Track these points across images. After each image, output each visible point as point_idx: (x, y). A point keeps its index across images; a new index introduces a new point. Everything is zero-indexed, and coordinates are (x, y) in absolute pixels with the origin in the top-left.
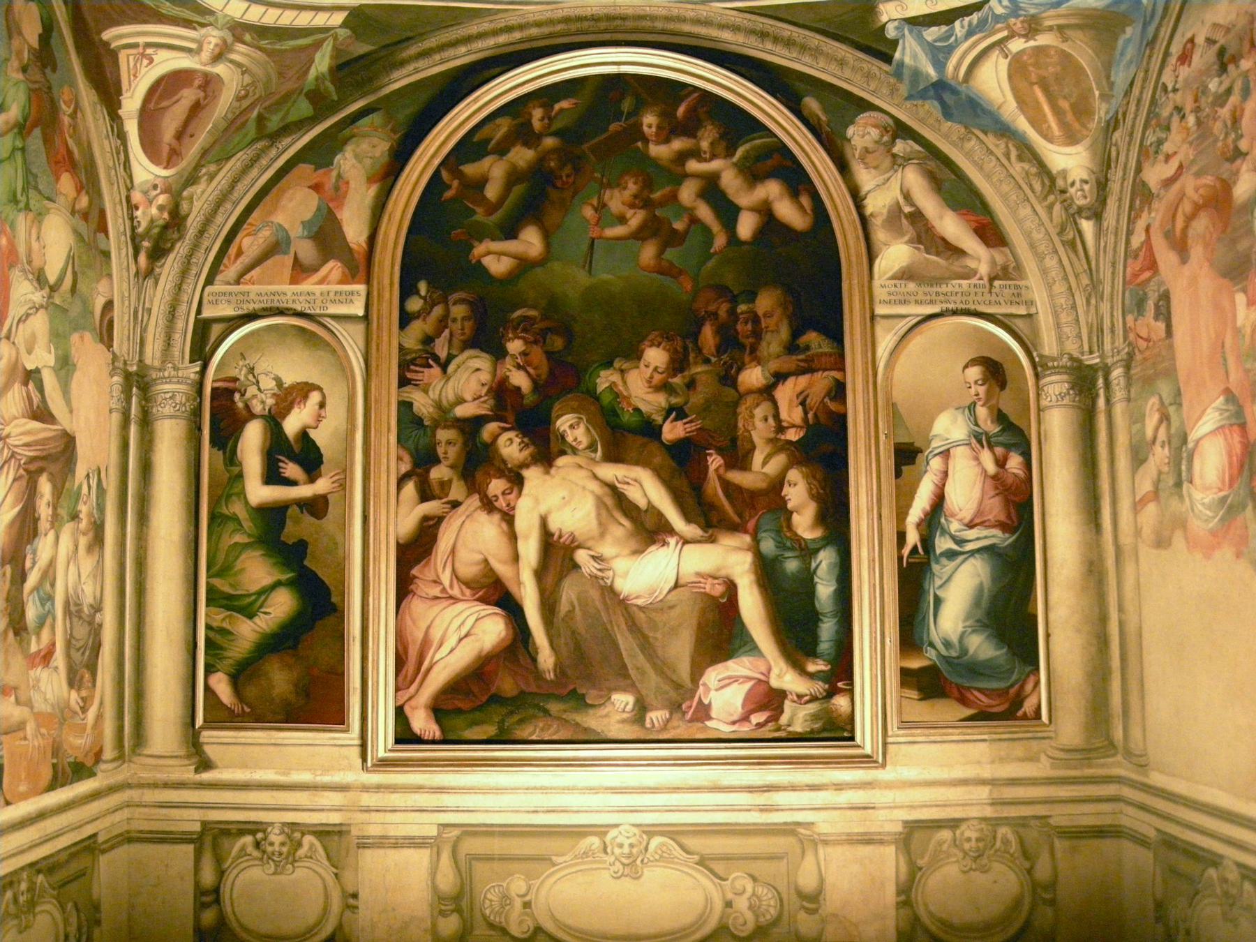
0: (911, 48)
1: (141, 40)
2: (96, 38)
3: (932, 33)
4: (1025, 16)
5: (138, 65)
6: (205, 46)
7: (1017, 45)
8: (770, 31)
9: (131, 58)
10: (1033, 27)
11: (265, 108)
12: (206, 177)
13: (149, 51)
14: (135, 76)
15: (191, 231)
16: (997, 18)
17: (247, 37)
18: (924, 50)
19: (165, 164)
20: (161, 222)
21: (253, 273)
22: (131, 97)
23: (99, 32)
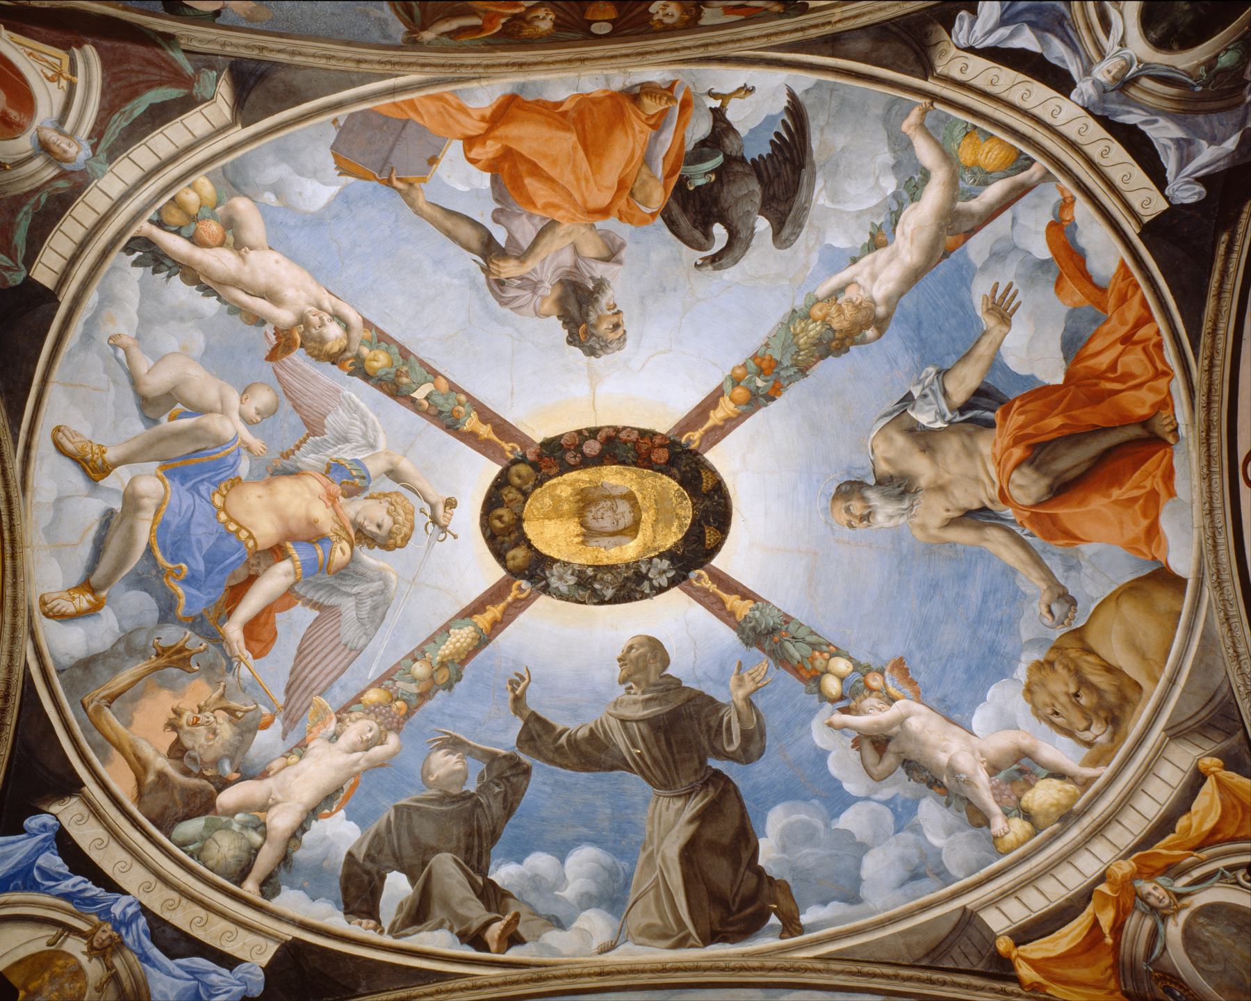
0: (19, 848)
3: (53, 861)
4: (120, 936)
7: (75, 947)
8: (9, 704)
10: (100, 952)
16: (106, 913)
18: (19, 862)
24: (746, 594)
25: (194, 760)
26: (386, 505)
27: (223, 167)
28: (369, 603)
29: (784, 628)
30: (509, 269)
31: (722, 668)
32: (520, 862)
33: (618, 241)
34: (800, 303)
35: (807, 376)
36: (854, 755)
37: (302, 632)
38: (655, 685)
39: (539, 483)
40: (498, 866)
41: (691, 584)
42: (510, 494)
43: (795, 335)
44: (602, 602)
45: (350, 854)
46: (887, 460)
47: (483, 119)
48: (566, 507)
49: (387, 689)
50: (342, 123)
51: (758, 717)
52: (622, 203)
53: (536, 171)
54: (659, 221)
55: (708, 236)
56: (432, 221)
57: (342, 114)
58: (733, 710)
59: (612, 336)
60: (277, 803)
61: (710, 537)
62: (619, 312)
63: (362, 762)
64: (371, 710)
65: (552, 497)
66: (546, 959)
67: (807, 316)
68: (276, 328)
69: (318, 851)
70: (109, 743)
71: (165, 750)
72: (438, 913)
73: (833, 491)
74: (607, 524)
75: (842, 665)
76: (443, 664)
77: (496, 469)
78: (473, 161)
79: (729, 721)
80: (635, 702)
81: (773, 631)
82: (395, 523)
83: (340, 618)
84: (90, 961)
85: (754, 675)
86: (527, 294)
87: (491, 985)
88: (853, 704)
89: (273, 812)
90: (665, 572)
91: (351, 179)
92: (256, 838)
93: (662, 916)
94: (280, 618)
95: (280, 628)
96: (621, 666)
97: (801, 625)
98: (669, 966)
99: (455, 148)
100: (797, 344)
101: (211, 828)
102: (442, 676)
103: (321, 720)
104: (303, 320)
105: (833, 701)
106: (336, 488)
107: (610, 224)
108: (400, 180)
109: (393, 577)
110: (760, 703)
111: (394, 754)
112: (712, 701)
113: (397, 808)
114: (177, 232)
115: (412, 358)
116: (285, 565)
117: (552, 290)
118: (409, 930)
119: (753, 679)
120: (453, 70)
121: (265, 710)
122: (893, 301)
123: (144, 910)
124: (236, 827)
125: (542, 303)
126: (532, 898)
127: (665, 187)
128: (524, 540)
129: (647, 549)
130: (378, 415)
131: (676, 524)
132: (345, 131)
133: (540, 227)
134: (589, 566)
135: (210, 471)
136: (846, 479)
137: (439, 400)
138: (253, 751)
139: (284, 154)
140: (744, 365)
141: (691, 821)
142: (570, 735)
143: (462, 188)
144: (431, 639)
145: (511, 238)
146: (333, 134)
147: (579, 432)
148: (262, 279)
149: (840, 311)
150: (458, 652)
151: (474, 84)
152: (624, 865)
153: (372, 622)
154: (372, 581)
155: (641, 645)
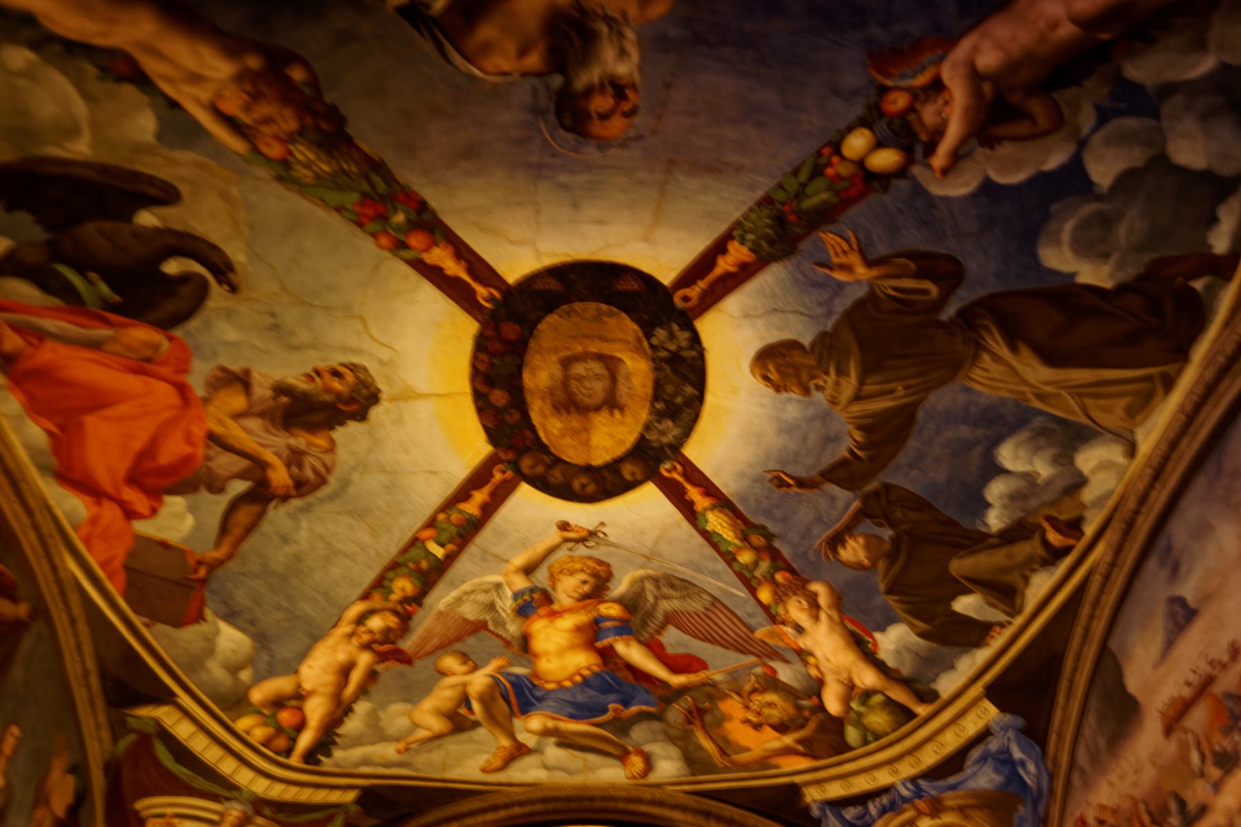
1: (169, 811)
3: (850, 813)
16: (904, 800)
17: (267, 811)
24: (719, 248)
25: (792, 720)
26: (562, 577)
27: (222, 710)
28: (666, 590)
29: (779, 206)
30: (280, 476)
31: (818, 285)
32: (988, 505)
33: (219, 374)
34: (262, 172)
35: (382, 160)
36: (1006, 149)
37: (686, 637)
38: (820, 360)
39: (544, 449)
40: (986, 525)
41: (692, 309)
42: (557, 475)
43: (318, 177)
44: (700, 398)
45: (922, 635)
46: (522, 52)
47: (99, 503)
48: (575, 424)
49: (760, 583)
50: (146, 620)
51: (900, 255)
52: (165, 371)
53: (149, 452)
54: (178, 333)
55: (185, 279)
56: (236, 545)
57: (137, 620)
58: (880, 282)
59: (350, 377)
60: (851, 680)
61: (632, 285)
62: (318, 372)
63: (829, 612)
64: (780, 598)
65: (563, 436)
66: (1111, 503)
67: (285, 163)
68: (378, 662)
69: (908, 658)
70: (764, 762)
71: (776, 734)
72: (1015, 578)
73: (570, 137)
74: (598, 388)
75: (857, 143)
76: (745, 538)
77: (525, 490)
78: (154, 511)
79: (895, 289)
80: (837, 384)
81: (780, 220)
82: (582, 570)
83: (678, 611)
84: (939, 818)
85: (839, 250)
86: (309, 461)
87: (1113, 565)
88: (924, 137)
89: (858, 682)
90: (672, 336)
91: (208, 613)
92: (878, 699)
93: (1121, 395)
94: (670, 650)
95: (681, 651)
96: (786, 390)
97: (780, 186)
98: (1189, 408)
99: (143, 527)
100: (333, 176)
101: (859, 723)
102: (757, 540)
103: (781, 636)
104: (367, 647)
105: (910, 161)
106: (542, 611)
107: (197, 381)
108: (196, 571)
109: (641, 572)
110: (882, 250)
111: (831, 589)
112: (860, 305)
113: (890, 591)
114: (294, 740)
115: (401, 560)
116: (620, 648)
117: (297, 436)
118: (1018, 601)
119: (845, 252)
120: (49, 541)
121: (759, 670)
122: (231, 46)
123: (913, 780)
124: (862, 709)
125: (317, 446)
126: (1033, 503)
127: (124, 326)
128: (614, 466)
129: (638, 349)
130: (464, 582)
131: (606, 319)
132: (155, 617)
133: (219, 449)
134: (652, 405)
135: (523, 691)
136: (552, 118)
137: (444, 537)
138: (795, 684)
139: (195, 663)
140: (374, 235)
141: (1014, 349)
142: (860, 448)
143: (189, 521)
144: (715, 546)
145: (242, 476)
146: (161, 628)
147: (480, 411)
148: (330, 679)
149: (268, 120)
150: (734, 527)
151: (59, 512)
152: (1037, 422)
153: (685, 588)
154: (643, 589)
155: (765, 367)
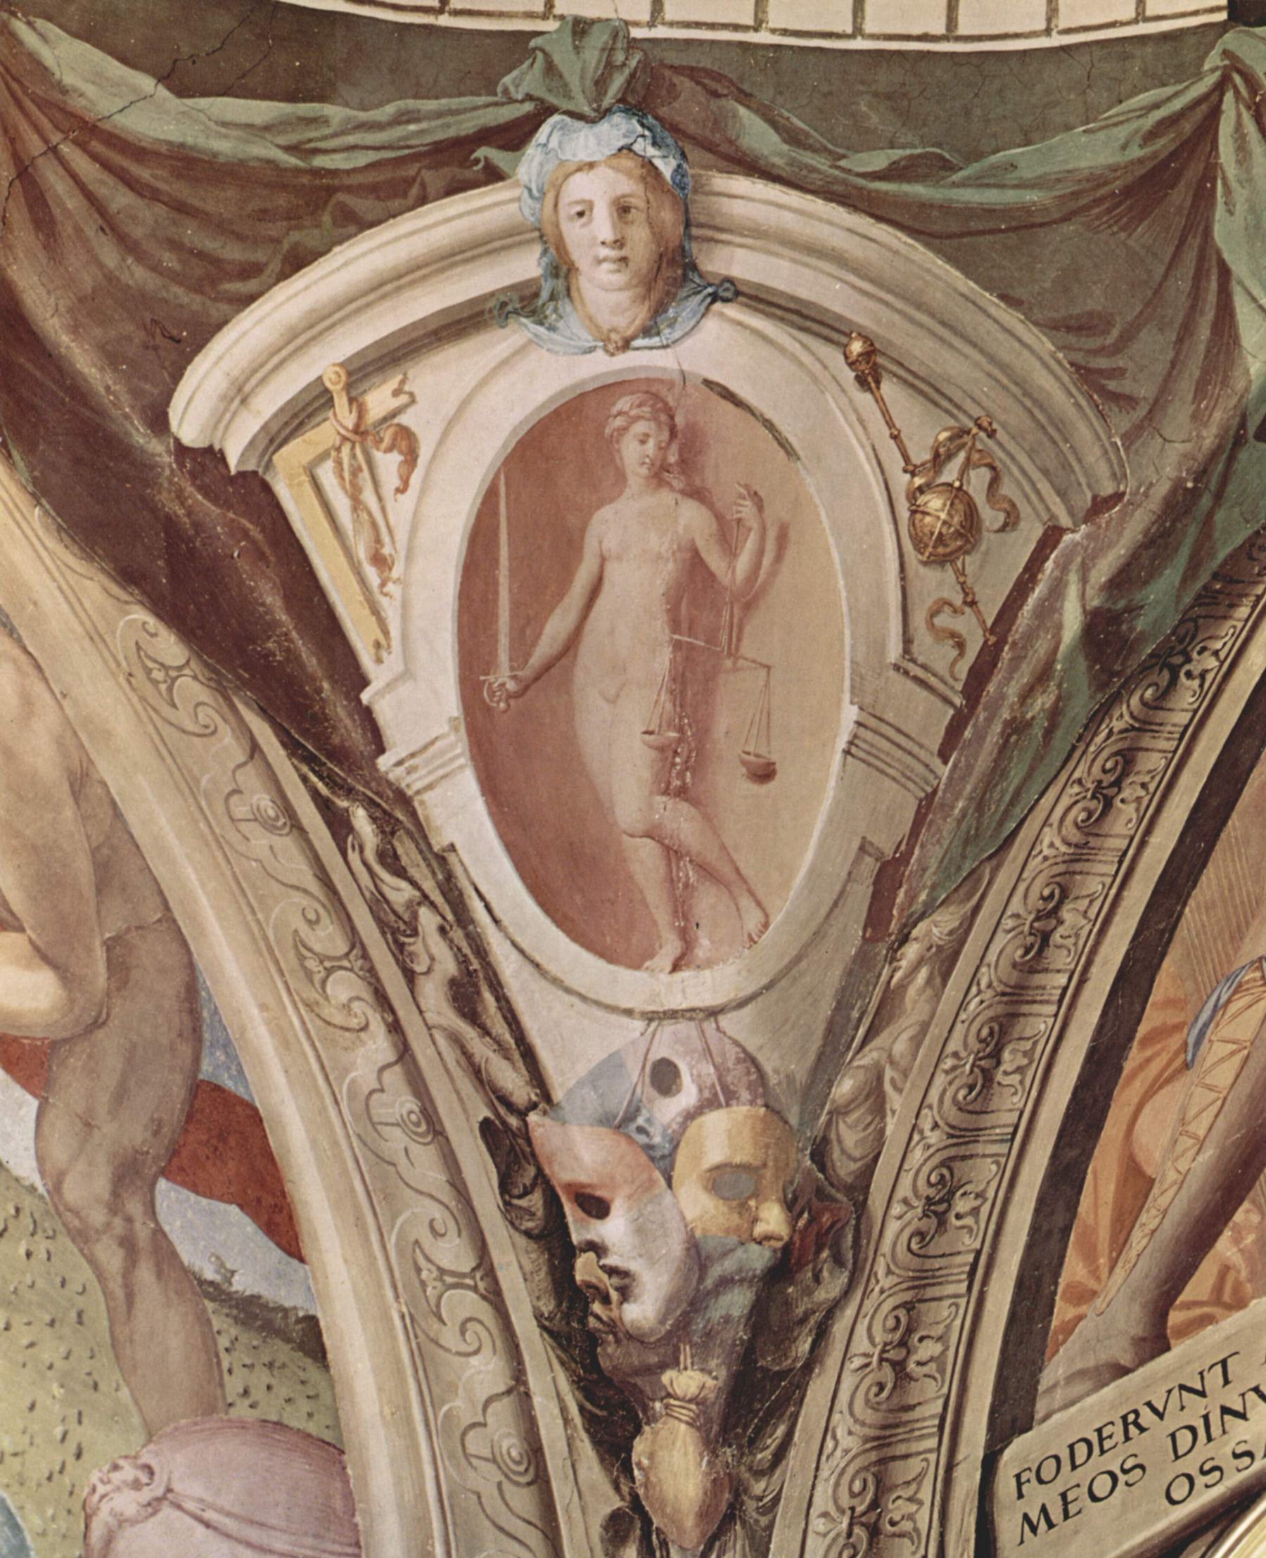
2: (156, 448)
5: (369, 497)
6: (573, 233)
9: (326, 474)
11: (1121, 581)
12: (923, 973)
13: (379, 400)
14: (380, 561)
15: (893, 1227)
19: (670, 947)
20: (758, 1259)
21: (1225, 1247)
22: (407, 674)
23: (159, 421)
